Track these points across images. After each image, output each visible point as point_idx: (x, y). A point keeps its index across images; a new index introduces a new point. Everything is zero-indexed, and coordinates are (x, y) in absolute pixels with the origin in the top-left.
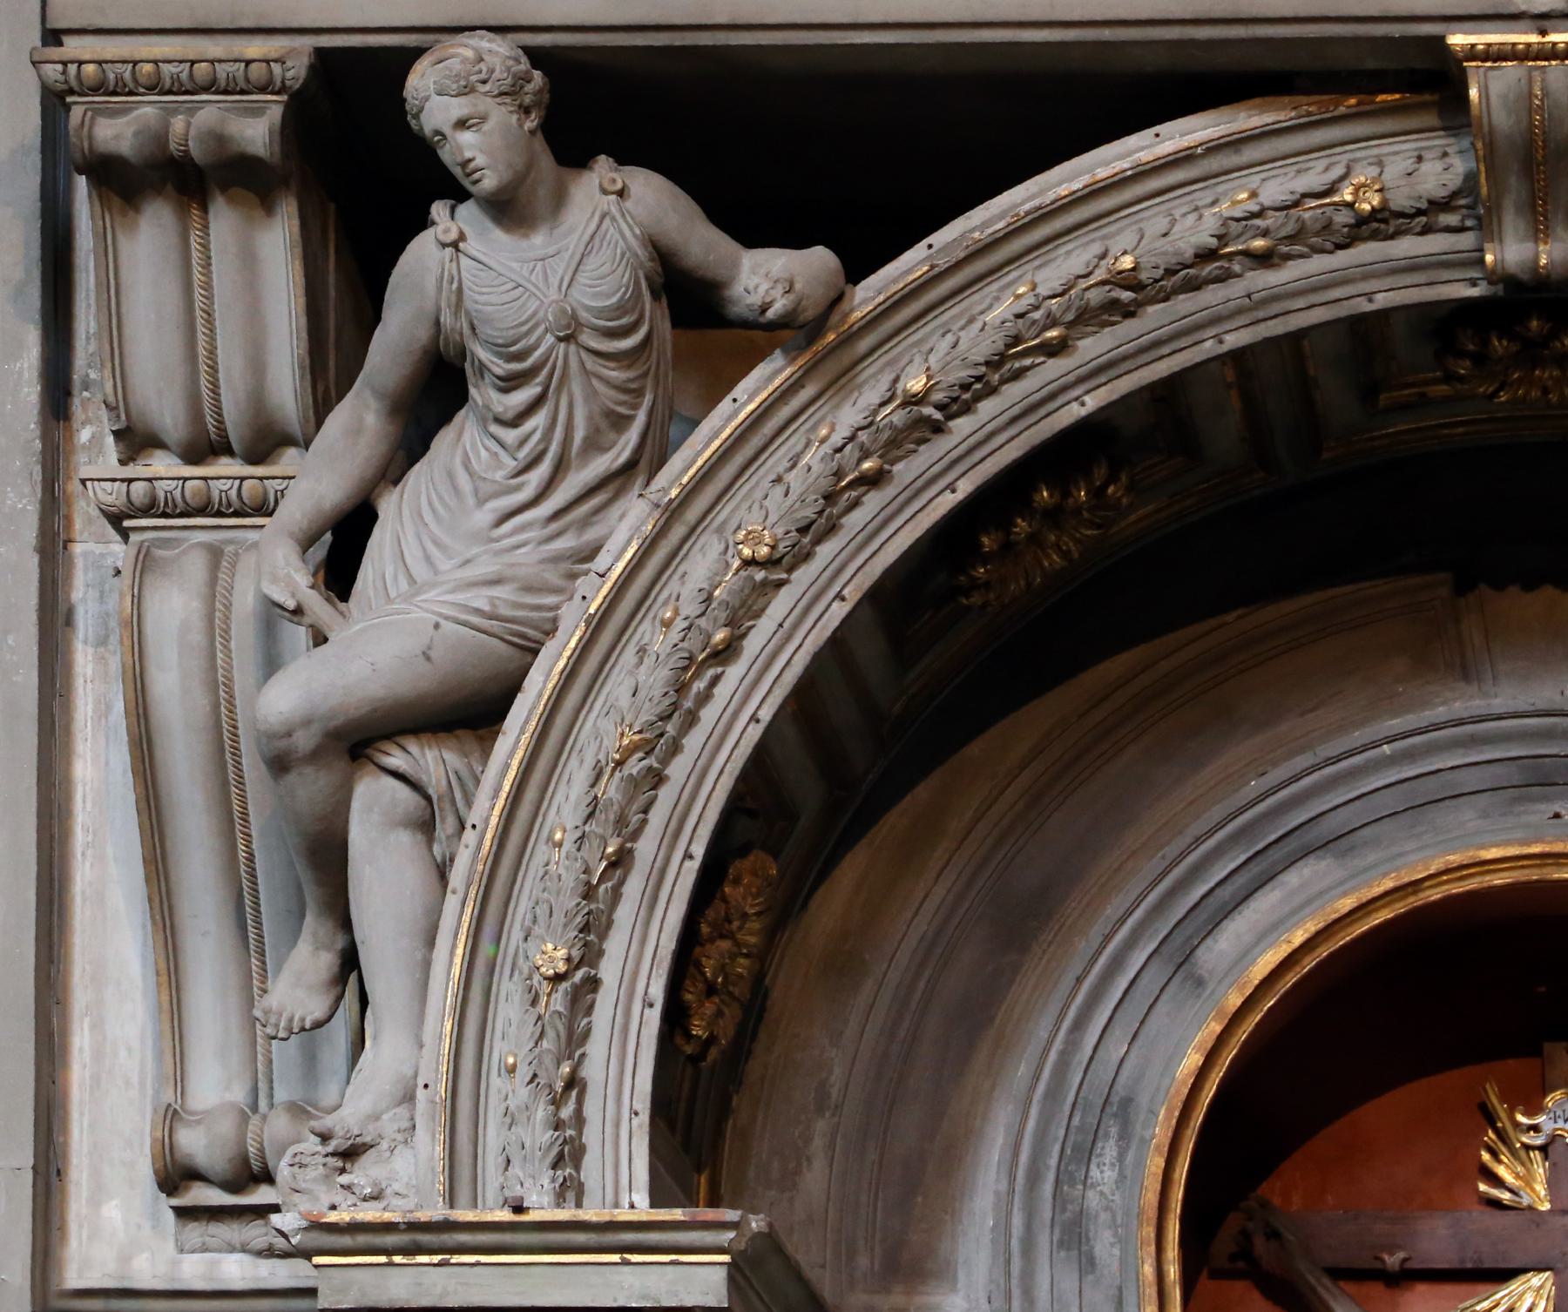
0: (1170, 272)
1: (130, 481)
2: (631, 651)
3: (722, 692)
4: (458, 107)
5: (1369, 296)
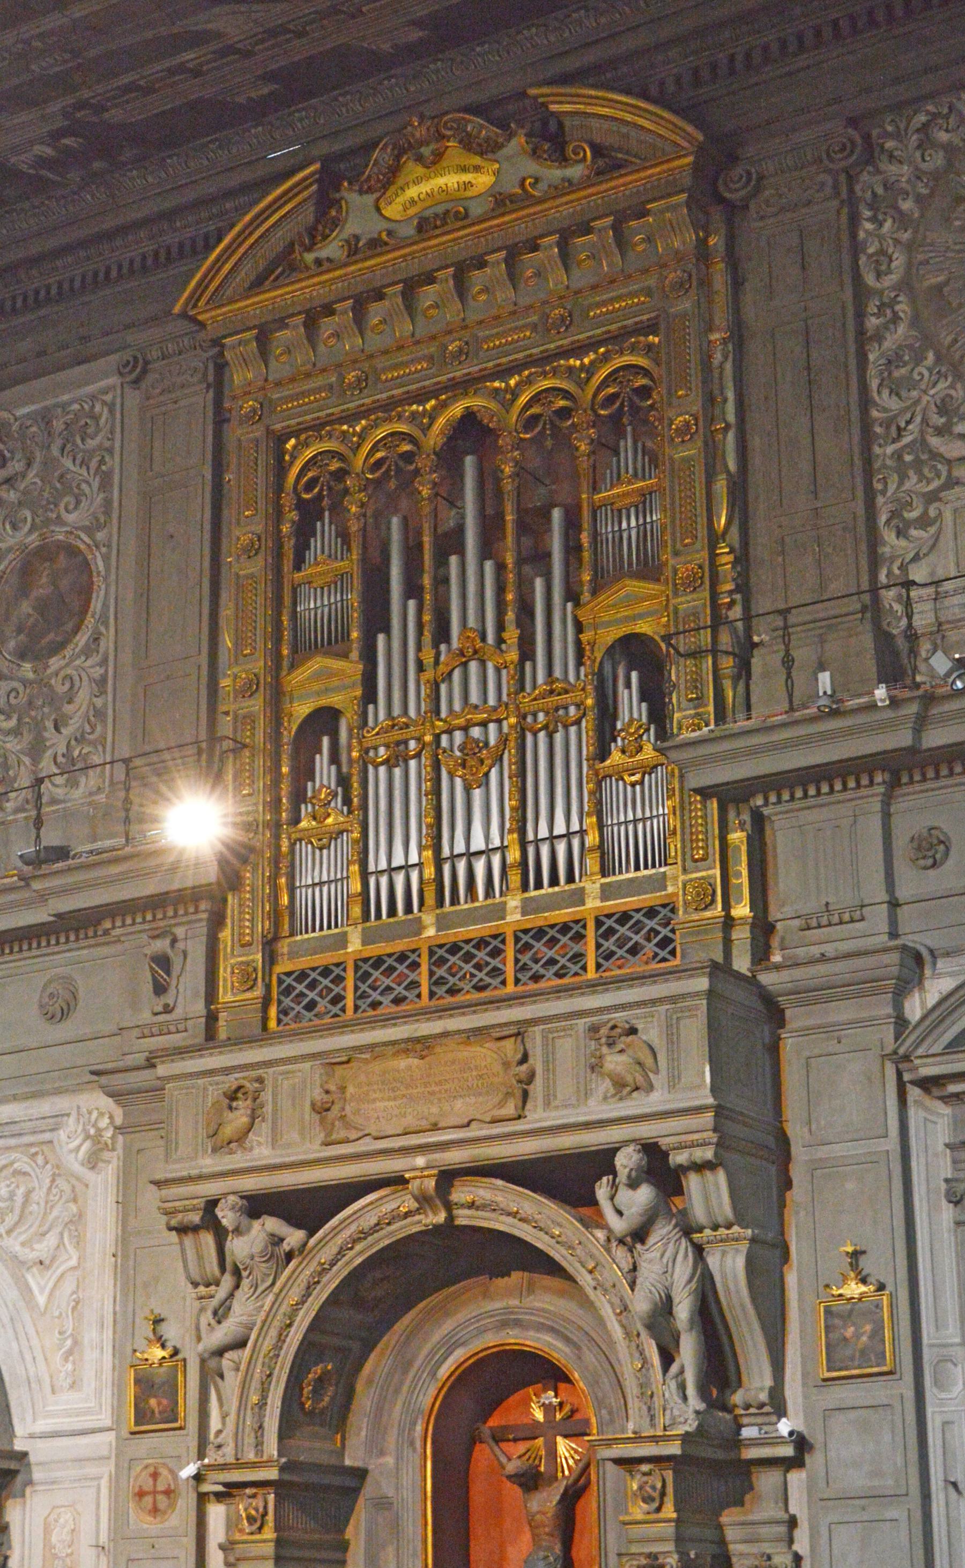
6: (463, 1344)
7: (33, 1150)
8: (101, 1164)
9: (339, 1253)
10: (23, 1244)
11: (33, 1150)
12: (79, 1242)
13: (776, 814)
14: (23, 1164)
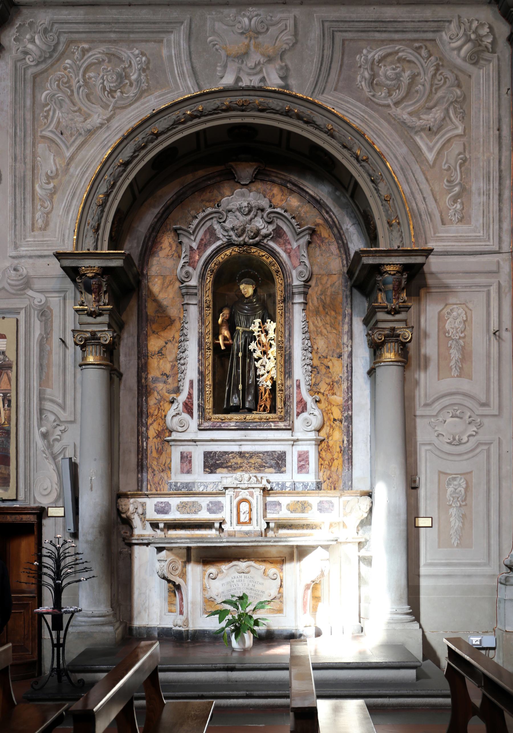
7: (417, 45)
8: (482, 62)
10: (410, 114)
11: (417, 45)
12: (464, 117)
14: (407, 53)
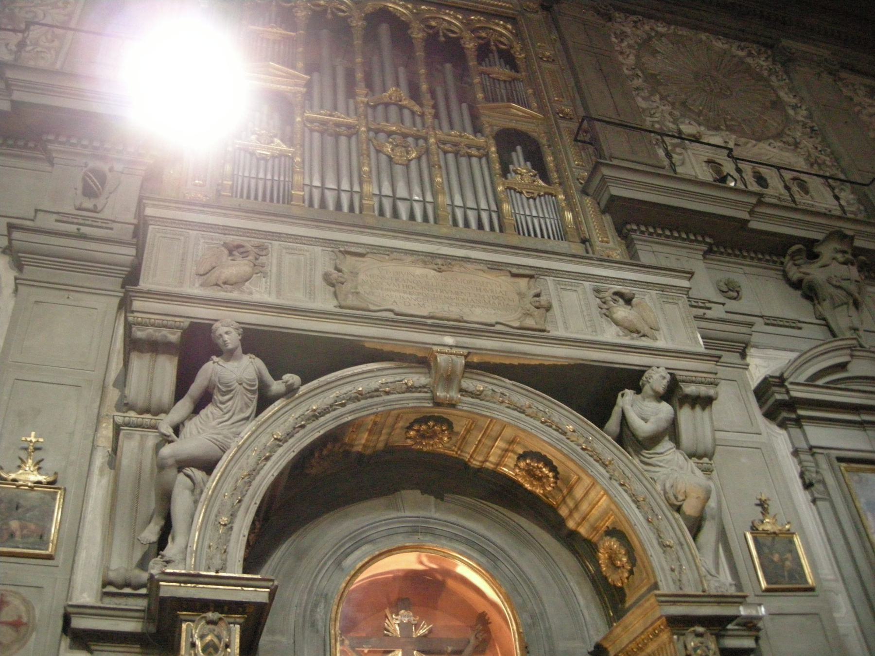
0: (369, 393)
1: (125, 417)
2: (246, 456)
3: (266, 468)
4: (226, 329)
5: (408, 404)
6: (371, 542)
9: (331, 406)
13: (640, 240)
